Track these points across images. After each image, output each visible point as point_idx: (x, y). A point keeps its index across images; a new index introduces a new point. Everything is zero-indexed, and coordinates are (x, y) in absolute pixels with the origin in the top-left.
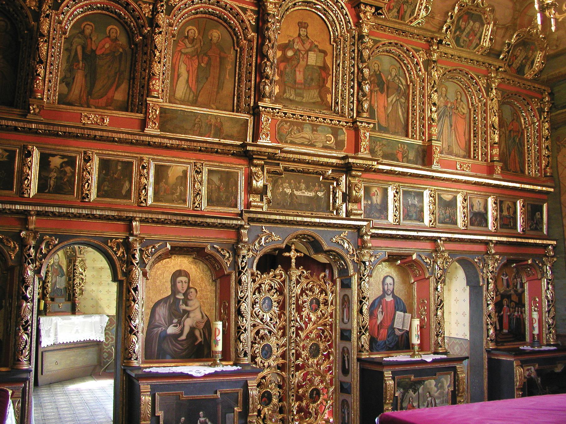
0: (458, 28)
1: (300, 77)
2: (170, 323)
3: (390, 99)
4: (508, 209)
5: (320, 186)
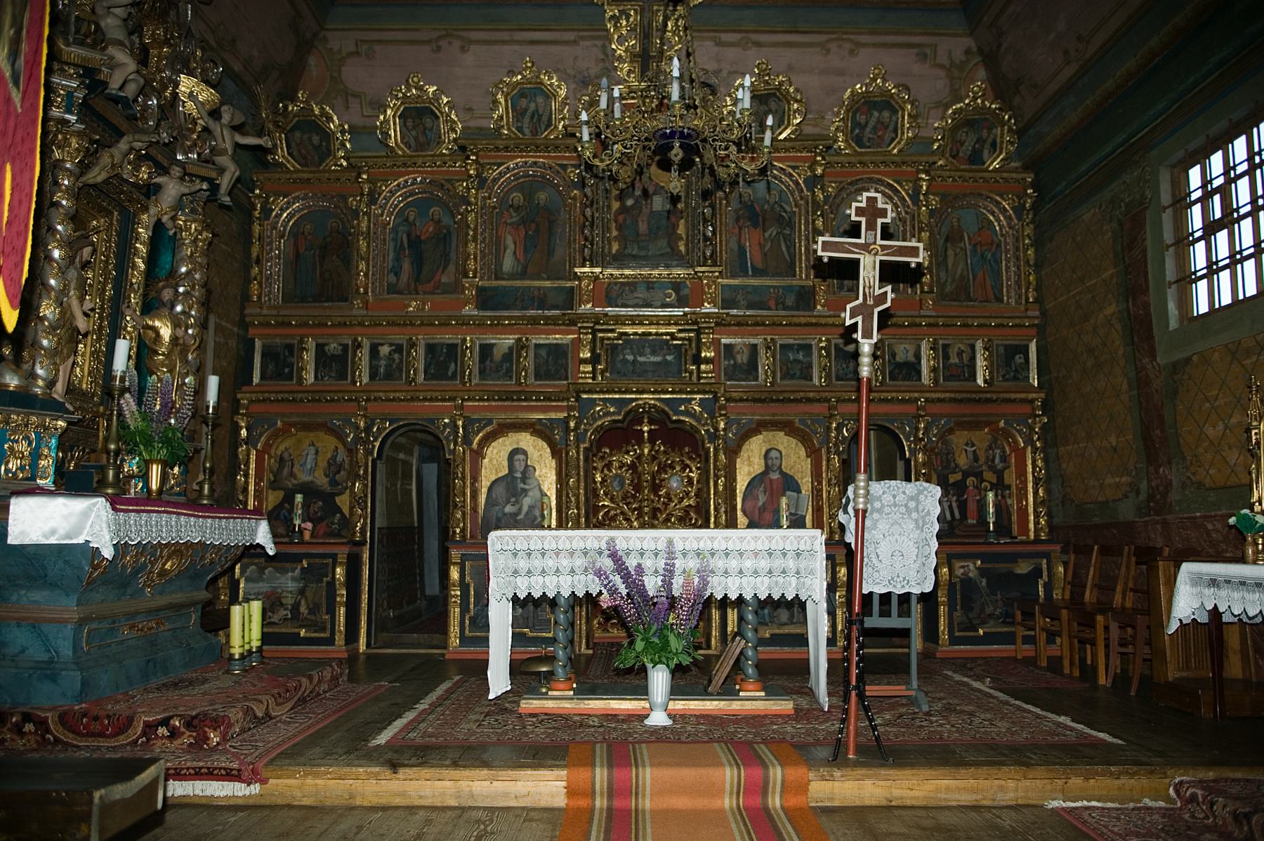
0: (856, 124)
1: (643, 227)
2: (508, 502)
3: (767, 235)
4: (960, 354)
5: (669, 348)
